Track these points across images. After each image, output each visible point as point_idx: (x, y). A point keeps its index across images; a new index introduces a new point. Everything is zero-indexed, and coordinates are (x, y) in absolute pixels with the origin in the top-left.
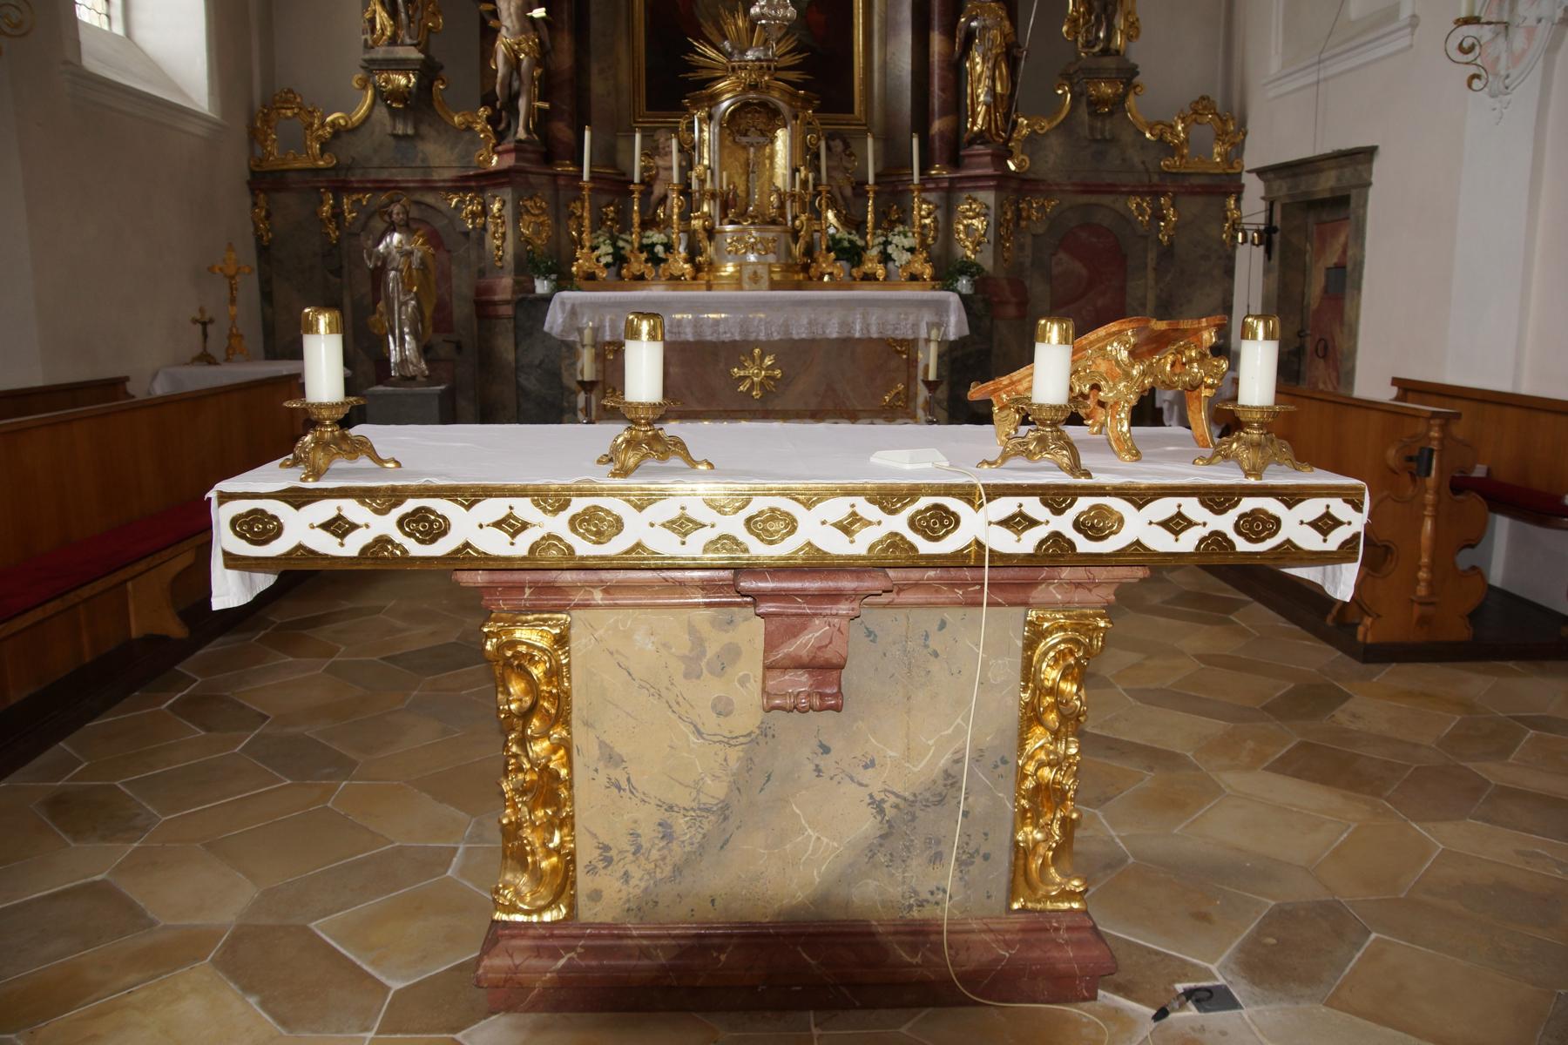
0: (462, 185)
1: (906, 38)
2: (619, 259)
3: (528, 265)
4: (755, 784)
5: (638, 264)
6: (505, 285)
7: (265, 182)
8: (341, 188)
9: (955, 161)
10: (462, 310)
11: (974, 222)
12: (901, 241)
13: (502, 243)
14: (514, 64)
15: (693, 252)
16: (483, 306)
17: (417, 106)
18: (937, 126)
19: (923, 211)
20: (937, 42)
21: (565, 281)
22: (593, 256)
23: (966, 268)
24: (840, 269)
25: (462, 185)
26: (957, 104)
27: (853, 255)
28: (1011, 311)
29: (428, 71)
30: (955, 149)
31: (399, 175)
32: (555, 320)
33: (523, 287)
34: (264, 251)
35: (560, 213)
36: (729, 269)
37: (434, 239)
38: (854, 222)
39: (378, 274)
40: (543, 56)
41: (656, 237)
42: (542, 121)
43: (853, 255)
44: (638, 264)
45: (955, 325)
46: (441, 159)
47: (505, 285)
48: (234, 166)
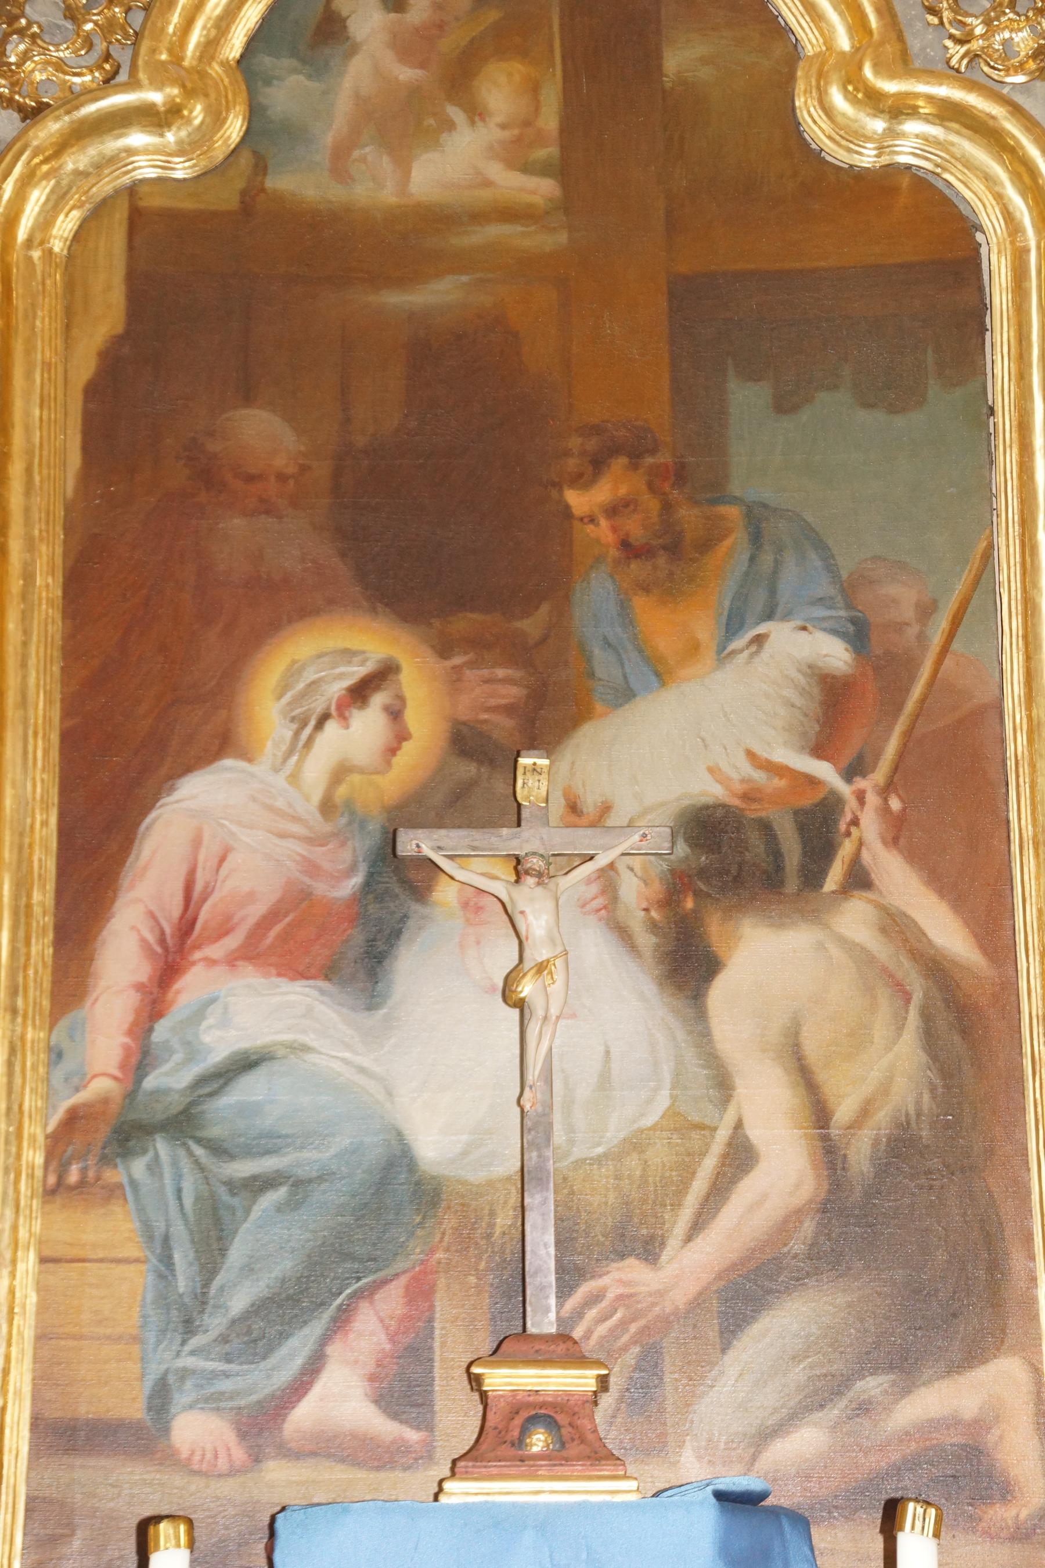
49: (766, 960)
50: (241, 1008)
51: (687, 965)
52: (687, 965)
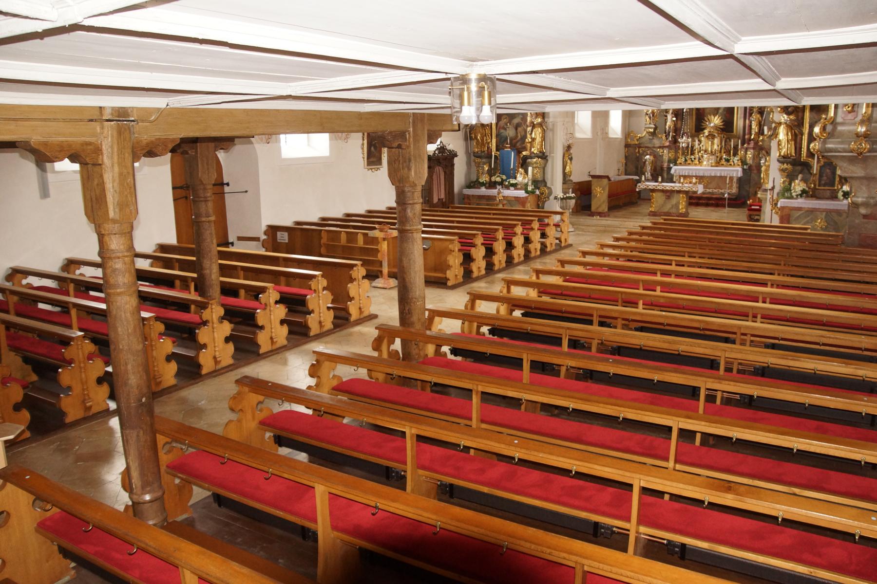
0: (660, 147)
1: (742, 120)
2: (686, 160)
3: (669, 161)
4: (665, 202)
5: (689, 162)
6: (665, 165)
7: (627, 146)
8: (639, 147)
9: (749, 144)
10: (658, 168)
11: (750, 155)
12: (736, 158)
13: (666, 158)
14: (670, 127)
15: (699, 159)
16: (662, 168)
17: (653, 134)
18: (747, 137)
19: (741, 153)
20: (747, 121)
21: (676, 164)
22: (681, 160)
23: (747, 164)
24: (725, 163)
25: (660, 147)
26: (750, 134)
27: (728, 161)
28: (755, 172)
29: (655, 129)
30: (750, 140)
31: (650, 145)
32: (672, 171)
33: (669, 165)
34: (626, 157)
35: (676, 152)
36: (705, 163)
37: (655, 157)
38: (729, 155)
39: (645, 163)
40: (675, 125)
41: (693, 157)
42: (673, 137)
43: (728, 161)
44: (689, 162)
45: (740, 174)
46: (657, 142)
47: (665, 165)
48: (623, 144)
49: (519, 129)
50: (502, 131)
51: (516, 129)
52: (516, 129)
